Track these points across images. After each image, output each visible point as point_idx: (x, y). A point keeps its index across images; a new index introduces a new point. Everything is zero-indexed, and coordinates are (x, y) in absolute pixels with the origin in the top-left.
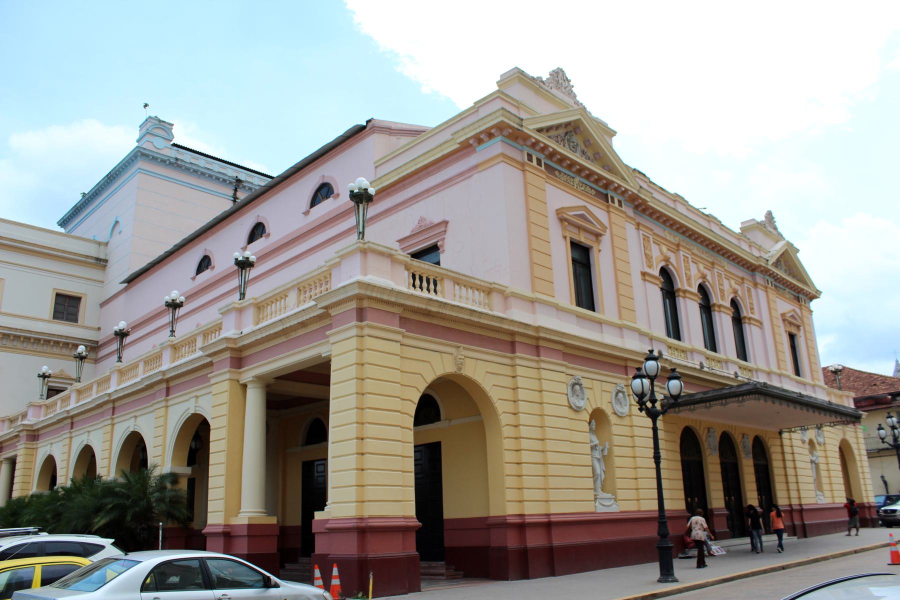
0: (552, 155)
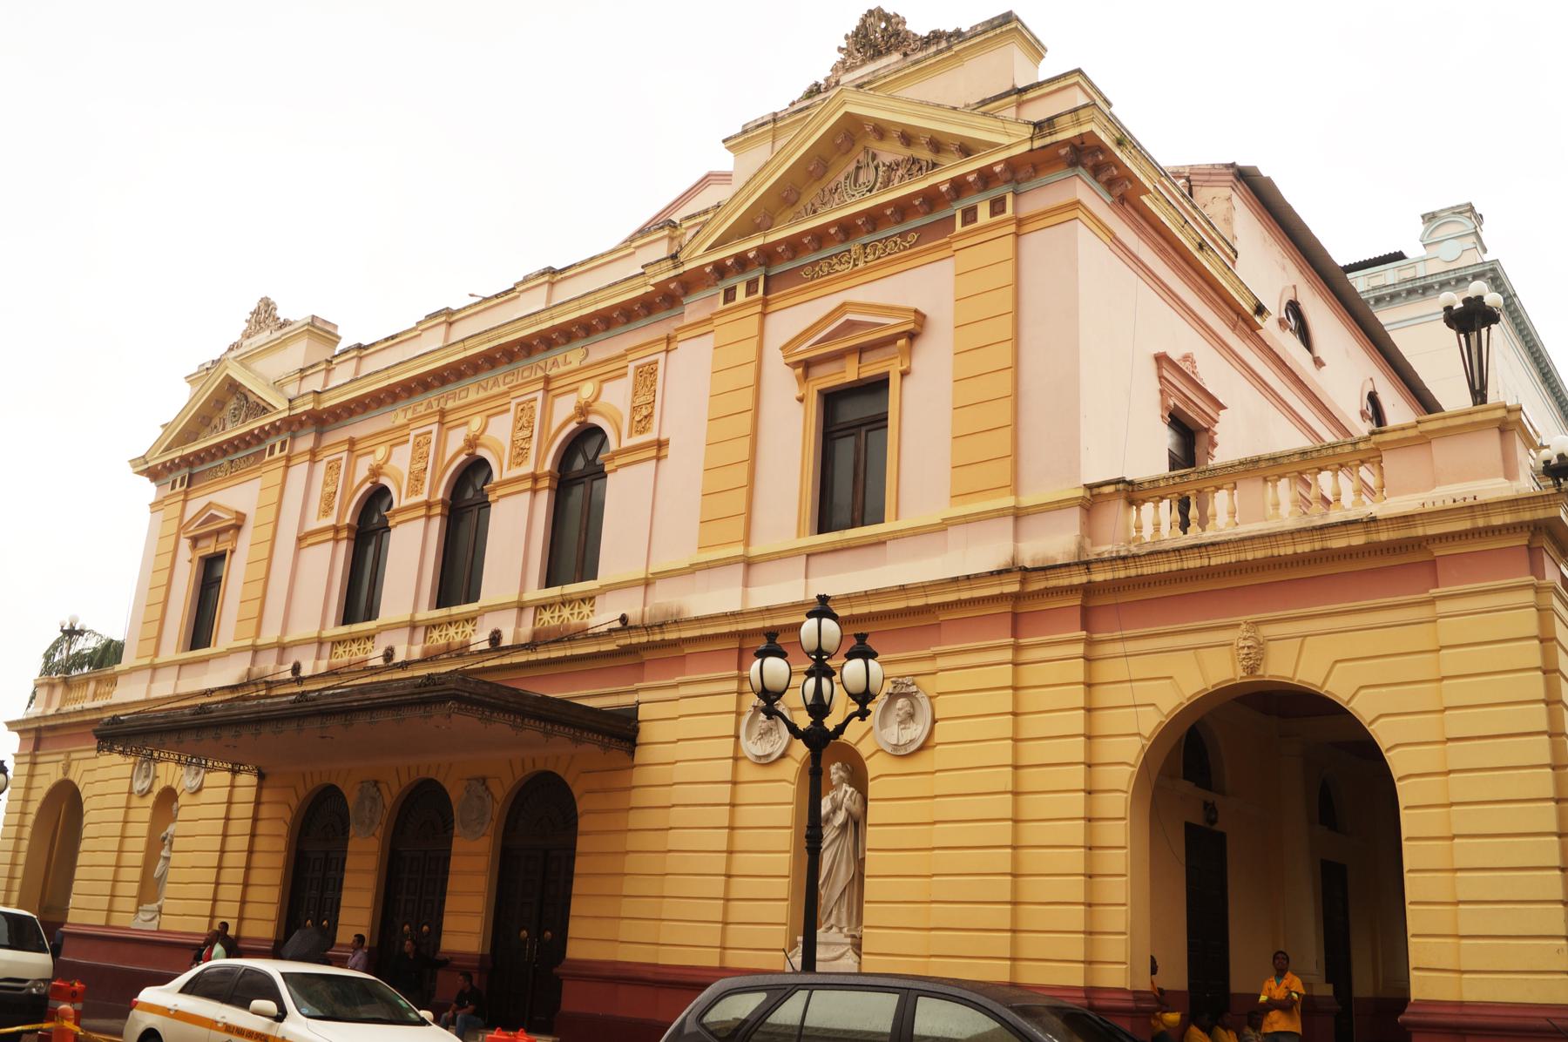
0: (768, 255)
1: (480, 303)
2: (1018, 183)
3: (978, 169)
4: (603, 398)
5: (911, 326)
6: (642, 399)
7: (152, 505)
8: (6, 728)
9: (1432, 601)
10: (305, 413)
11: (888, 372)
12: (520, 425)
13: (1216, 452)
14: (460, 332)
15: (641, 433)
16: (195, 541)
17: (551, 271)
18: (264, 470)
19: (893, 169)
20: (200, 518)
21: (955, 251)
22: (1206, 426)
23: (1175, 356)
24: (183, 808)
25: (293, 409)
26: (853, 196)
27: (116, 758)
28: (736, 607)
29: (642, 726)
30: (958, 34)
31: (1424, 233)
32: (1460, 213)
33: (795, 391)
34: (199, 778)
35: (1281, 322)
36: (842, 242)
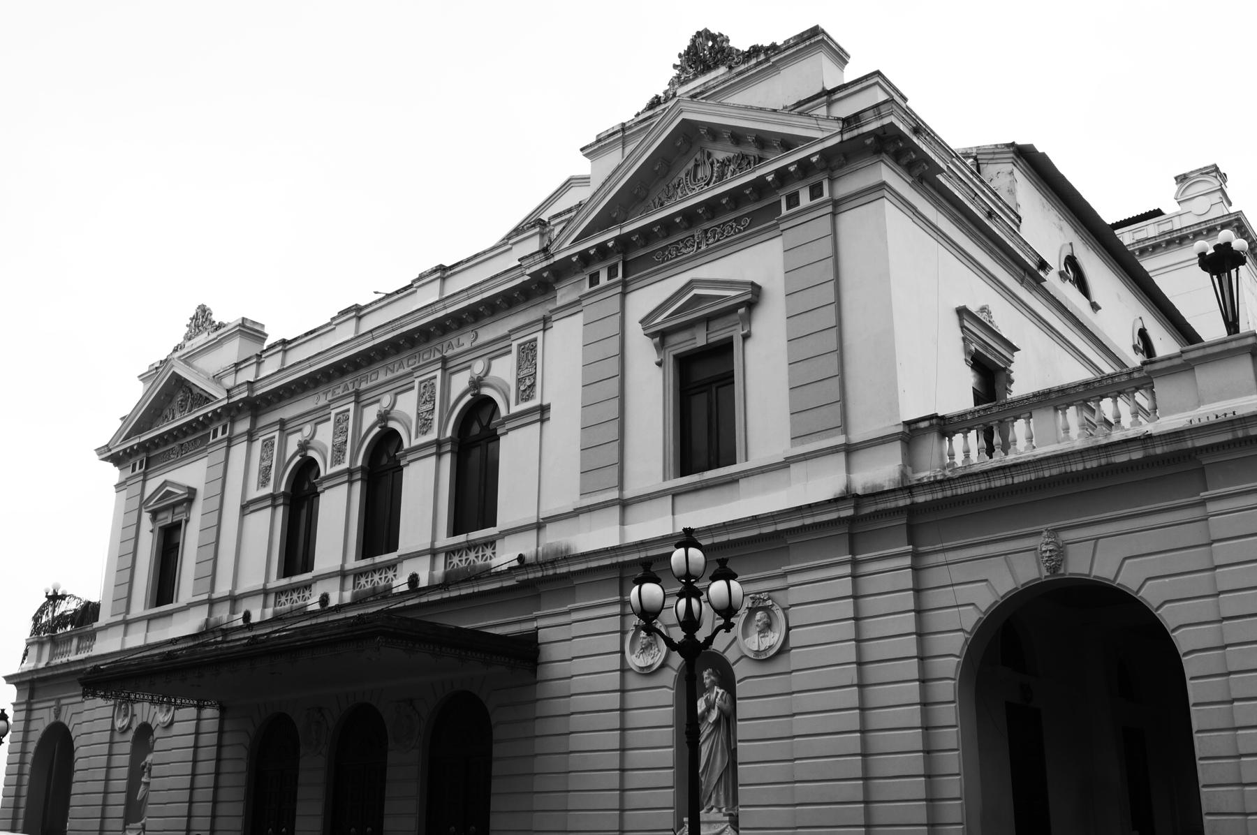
0: (624, 243)
1: (383, 299)
2: (832, 170)
3: (798, 161)
4: (493, 373)
5: (749, 296)
6: (525, 372)
7: (117, 486)
8: (4, 681)
9: (1203, 503)
10: (241, 400)
11: (732, 337)
12: (423, 400)
13: (1013, 387)
14: (369, 323)
15: (526, 400)
16: (155, 514)
17: (441, 269)
18: (209, 450)
19: (726, 165)
20: (157, 495)
21: (782, 231)
22: (1003, 366)
23: (973, 308)
24: (158, 740)
25: (231, 398)
26: (694, 189)
27: (100, 701)
28: (615, 542)
29: (542, 648)
30: (774, 47)
31: (1179, 189)
32: (1207, 173)
33: (654, 357)
34: (170, 714)
35: (1062, 275)
36: (686, 229)
